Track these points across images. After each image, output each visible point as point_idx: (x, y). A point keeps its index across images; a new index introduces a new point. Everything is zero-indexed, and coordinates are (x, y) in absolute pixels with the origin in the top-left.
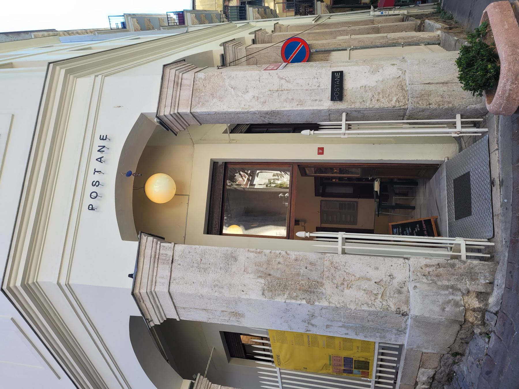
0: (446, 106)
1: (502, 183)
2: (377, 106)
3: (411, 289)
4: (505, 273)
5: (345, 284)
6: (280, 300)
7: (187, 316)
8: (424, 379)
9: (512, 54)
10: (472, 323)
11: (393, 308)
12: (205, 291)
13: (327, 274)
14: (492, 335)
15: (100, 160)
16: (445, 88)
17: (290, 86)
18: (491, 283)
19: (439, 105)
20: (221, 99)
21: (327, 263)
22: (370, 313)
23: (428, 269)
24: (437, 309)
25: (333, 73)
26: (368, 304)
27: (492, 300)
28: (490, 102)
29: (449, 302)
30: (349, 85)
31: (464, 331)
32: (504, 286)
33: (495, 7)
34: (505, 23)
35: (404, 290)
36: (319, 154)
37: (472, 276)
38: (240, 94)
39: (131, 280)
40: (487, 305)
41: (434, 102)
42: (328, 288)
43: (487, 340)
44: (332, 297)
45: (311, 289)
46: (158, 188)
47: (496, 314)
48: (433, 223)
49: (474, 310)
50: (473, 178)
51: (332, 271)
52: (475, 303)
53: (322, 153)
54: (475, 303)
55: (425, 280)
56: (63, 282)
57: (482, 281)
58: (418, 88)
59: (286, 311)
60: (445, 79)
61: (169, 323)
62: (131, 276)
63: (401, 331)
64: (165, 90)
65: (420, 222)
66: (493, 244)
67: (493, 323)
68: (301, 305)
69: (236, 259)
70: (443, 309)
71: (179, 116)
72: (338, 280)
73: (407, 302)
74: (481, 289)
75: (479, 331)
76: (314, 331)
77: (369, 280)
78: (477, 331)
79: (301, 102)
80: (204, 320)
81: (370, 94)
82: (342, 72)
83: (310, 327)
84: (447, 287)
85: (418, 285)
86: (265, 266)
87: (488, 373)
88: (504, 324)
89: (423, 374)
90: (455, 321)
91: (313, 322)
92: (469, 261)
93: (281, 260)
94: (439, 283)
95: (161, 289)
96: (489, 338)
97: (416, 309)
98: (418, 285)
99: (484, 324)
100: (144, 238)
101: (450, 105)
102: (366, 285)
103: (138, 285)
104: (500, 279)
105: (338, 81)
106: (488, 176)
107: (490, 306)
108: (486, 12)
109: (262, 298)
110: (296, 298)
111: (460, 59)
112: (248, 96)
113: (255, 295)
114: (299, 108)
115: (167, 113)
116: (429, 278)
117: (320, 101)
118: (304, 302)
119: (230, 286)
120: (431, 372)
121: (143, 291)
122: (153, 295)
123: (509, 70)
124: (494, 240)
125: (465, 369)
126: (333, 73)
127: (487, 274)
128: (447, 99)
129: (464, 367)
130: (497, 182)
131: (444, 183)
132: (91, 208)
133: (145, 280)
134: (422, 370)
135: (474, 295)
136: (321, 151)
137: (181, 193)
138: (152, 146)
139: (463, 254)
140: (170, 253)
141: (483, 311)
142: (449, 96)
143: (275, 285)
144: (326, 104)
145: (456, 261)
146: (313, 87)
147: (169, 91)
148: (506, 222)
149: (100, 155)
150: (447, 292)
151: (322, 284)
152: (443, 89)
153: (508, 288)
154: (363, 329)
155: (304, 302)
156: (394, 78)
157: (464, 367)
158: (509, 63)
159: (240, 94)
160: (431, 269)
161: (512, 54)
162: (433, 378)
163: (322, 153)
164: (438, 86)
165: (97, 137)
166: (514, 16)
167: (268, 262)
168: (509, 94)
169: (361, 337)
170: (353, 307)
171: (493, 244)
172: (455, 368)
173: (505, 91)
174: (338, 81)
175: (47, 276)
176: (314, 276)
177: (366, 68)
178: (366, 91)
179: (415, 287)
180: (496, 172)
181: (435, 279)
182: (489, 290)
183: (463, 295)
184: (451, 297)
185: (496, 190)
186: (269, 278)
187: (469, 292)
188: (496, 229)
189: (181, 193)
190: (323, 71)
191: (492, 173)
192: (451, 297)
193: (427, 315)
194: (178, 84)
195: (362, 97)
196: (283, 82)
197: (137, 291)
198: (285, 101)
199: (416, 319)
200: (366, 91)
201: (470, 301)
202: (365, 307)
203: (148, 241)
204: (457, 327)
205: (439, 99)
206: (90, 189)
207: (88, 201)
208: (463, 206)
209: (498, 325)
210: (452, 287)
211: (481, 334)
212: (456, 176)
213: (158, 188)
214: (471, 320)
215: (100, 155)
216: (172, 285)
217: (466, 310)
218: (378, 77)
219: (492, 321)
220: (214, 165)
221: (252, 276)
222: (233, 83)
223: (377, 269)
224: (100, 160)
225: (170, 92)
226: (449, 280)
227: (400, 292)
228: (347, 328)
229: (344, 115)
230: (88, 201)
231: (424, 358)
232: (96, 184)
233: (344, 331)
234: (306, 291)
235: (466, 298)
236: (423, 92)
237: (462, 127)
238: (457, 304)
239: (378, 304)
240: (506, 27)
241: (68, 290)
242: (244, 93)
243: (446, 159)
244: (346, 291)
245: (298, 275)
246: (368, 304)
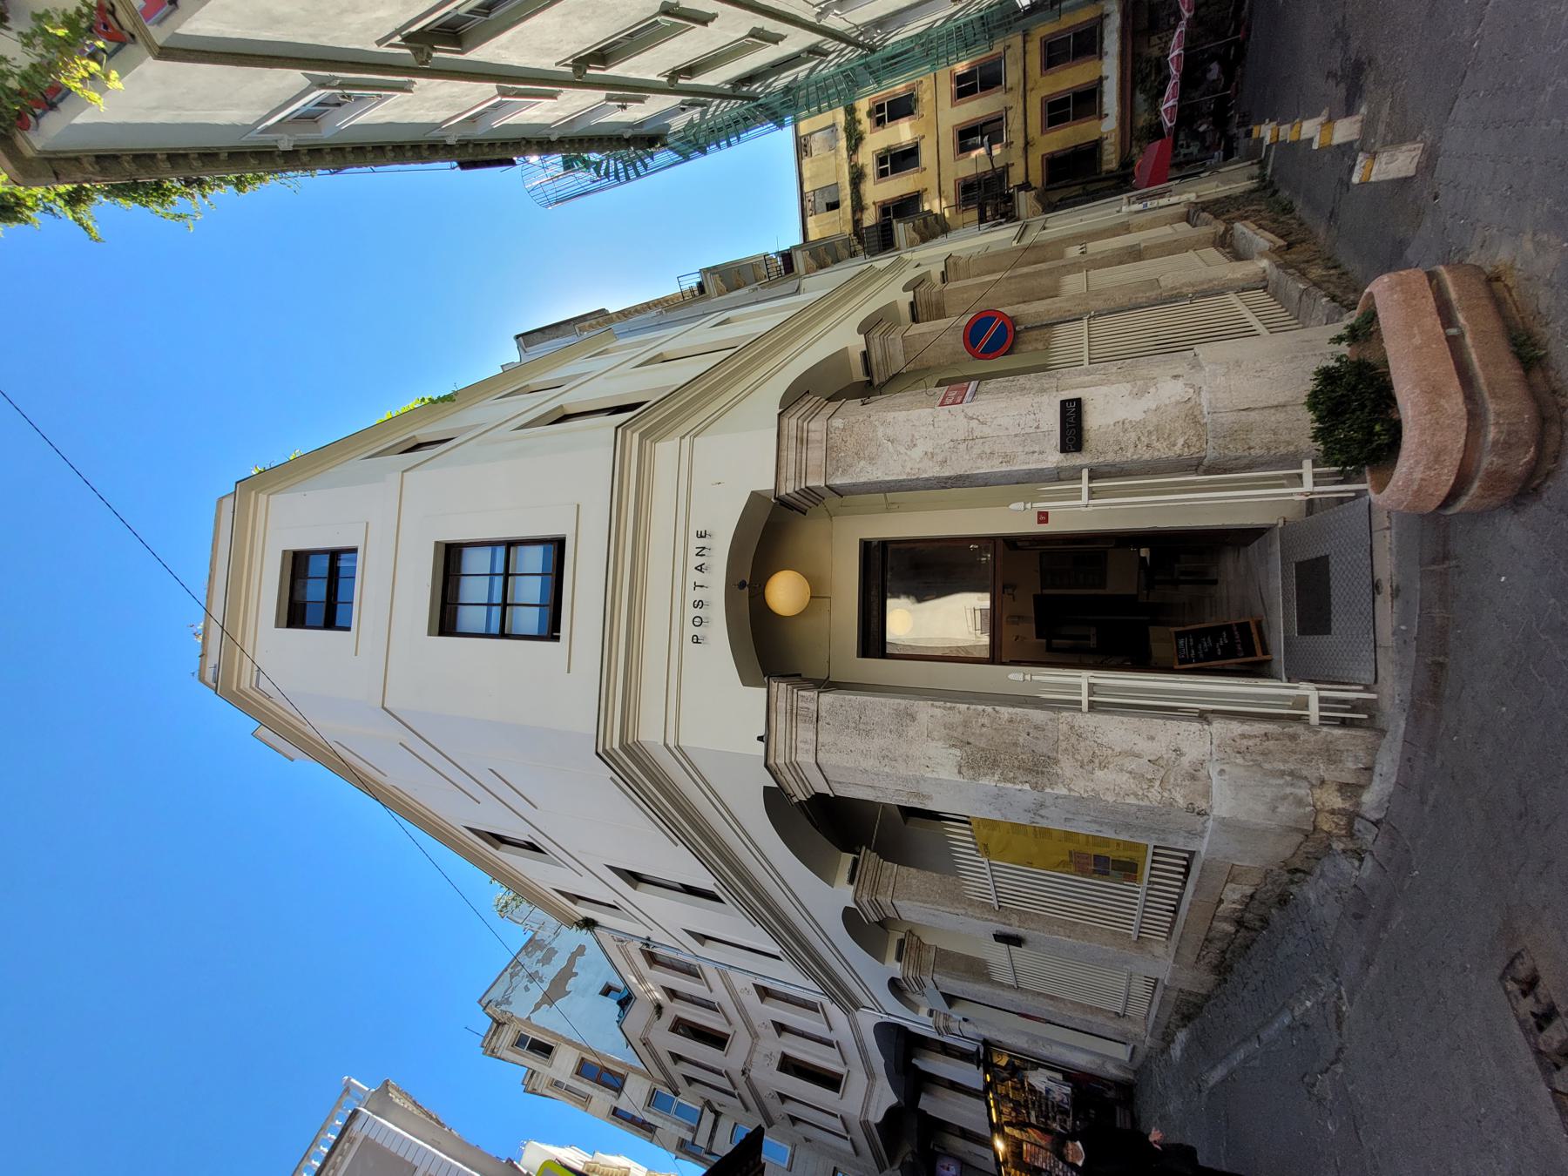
0: (1283, 450)
1: (1396, 593)
2: (1147, 456)
3: (1214, 774)
4: (1397, 756)
5: (1095, 761)
6: (989, 782)
7: (842, 792)
8: (1237, 897)
9: (1430, 412)
10: (1329, 833)
11: (1181, 802)
12: (869, 764)
13: (1064, 745)
14: (1368, 858)
15: (700, 568)
16: (1281, 416)
17: (987, 431)
18: (1369, 769)
19: (1269, 449)
20: (871, 460)
21: (1064, 728)
22: (1140, 808)
23: (1245, 742)
24: (1261, 808)
25: (1063, 403)
26: (1136, 795)
27: (1368, 798)
28: (1380, 487)
29: (1285, 798)
30: (1095, 421)
31: (1310, 850)
32: (1394, 780)
33: (1391, 288)
34: (1416, 330)
35: (1203, 772)
36: (1040, 522)
37: (1331, 755)
38: (903, 450)
39: (762, 745)
40: (1358, 804)
41: (1258, 444)
42: (1066, 766)
43: (1357, 864)
44: (1071, 782)
45: (1038, 768)
46: (784, 592)
47: (1376, 823)
48: (1254, 630)
49: (1333, 812)
50: (1335, 569)
51: (1073, 740)
52: (1337, 802)
53: (1046, 521)
54: (1337, 802)
55: (1240, 760)
56: (671, 745)
57: (1351, 765)
58: (1228, 418)
59: (997, 796)
60: (1281, 399)
61: (819, 799)
62: (760, 739)
63: (1193, 834)
64: (784, 454)
65: (1228, 628)
66: (1374, 696)
67: (1370, 838)
68: (1022, 791)
69: (913, 719)
70: (1274, 809)
71: (809, 492)
72: (1084, 755)
73: (1207, 794)
74: (1348, 778)
75: (1342, 846)
76: (1044, 823)
77: (1139, 756)
78: (1338, 846)
79: (1007, 458)
80: (871, 798)
81: (1133, 436)
82: (1078, 401)
83: (1038, 819)
84: (1282, 773)
85: (1225, 767)
86: (960, 729)
87: (1357, 916)
88: (1393, 846)
89: (1233, 891)
90: (1298, 830)
91: (1042, 812)
92: (1325, 729)
93: (986, 721)
94: (1267, 766)
95: (805, 758)
96: (1361, 860)
97: (1223, 804)
98: (1225, 767)
99: (1351, 835)
100: (774, 685)
101: (1292, 448)
102: (1132, 764)
103: (772, 752)
104: (1388, 763)
105: (1072, 417)
106: (1368, 572)
107: (1364, 808)
108: (1371, 295)
109: (959, 778)
110: (1013, 780)
111: (1313, 395)
112: (917, 453)
113: (948, 773)
114: (1005, 468)
115: (790, 491)
116: (1248, 757)
117: (1041, 453)
118: (1027, 787)
119: (907, 758)
120: (1249, 891)
121: (780, 761)
122: (795, 767)
123: (1422, 444)
124: (1376, 688)
125: (1312, 896)
126: (1063, 403)
127: (1361, 754)
128: (1285, 437)
129: (1310, 892)
130: (1386, 588)
131: (1276, 563)
132: (696, 640)
133: (781, 746)
134: (1229, 886)
135: (1334, 787)
136: (1043, 517)
137: (818, 594)
138: (770, 532)
139: (1314, 712)
140: (813, 707)
141: (1352, 816)
142: (1290, 430)
143: (979, 760)
144: (1054, 458)
145: (1298, 728)
146: (1028, 430)
147: (790, 455)
148: (1402, 666)
149: (700, 560)
150: (1281, 782)
151: (1057, 762)
152: (1275, 418)
153: (1403, 785)
154: (1128, 826)
155: (1027, 787)
156: (1178, 403)
157: (1310, 892)
158: (1423, 431)
159: (903, 450)
160: (1251, 743)
161: (1430, 412)
162: (1252, 897)
163: (1046, 521)
164: (1266, 412)
165: (692, 534)
166: (1434, 310)
167: (966, 724)
168: (1420, 487)
169: (1124, 837)
170: (1110, 798)
171: (1374, 696)
172: (1294, 889)
173: (1412, 481)
174: (1072, 417)
175: (650, 733)
176: (1043, 747)
177: (1125, 388)
178: (1125, 431)
179: (1222, 772)
180: (1385, 568)
181: (1260, 758)
182: (1362, 782)
183: (1313, 786)
184: (1288, 790)
185: (1384, 604)
186: (967, 748)
187: (1323, 782)
188: (1381, 671)
189: (818, 594)
190: (1045, 398)
191: (1376, 568)
192: (1288, 790)
193: (1243, 817)
194: (803, 441)
195: (1118, 442)
196: (974, 423)
197: (771, 762)
198: (980, 456)
199: (1223, 823)
200: (1125, 431)
201: (1325, 797)
202: (1131, 800)
203: (781, 688)
204: (1300, 838)
205: (1268, 437)
206: (691, 612)
207: (691, 630)
208: (1314, 612)
209: (1378, 843)
210: (1291, 774)
211: (1344, 851)
212: (1299, 558)
213: (784, 592)
214: (1326, 828)
215: (700, 560)
216: (820, 754)
217: (1317, 812)
218: (1148, 402)
219: (1368, 836)
220: (866, 547)
221: (940, 744)
222: (889, 432)
223: (1152, 738)
224: (700, 568)
225: (792, 456)
226: (1285, 762)
227: (1193, 778)
228: (1101, 824)
229: (1085, 473)
230: (691, 630)
231: (1235, 872)
232: (699, 604)
233: (1096, 827)
234: (1030, 771)
235: (1317, 792)
236: (1236, 427)
237: (1315, 484)
238: (1300, 802)
239: (1155, 794)
240: (1417, 341)
241: (679, 753)
242: (909, 448)
243: (1281, 523)
244: (1099, 773)
245: (1015, 744)
246: (1136, 795)
